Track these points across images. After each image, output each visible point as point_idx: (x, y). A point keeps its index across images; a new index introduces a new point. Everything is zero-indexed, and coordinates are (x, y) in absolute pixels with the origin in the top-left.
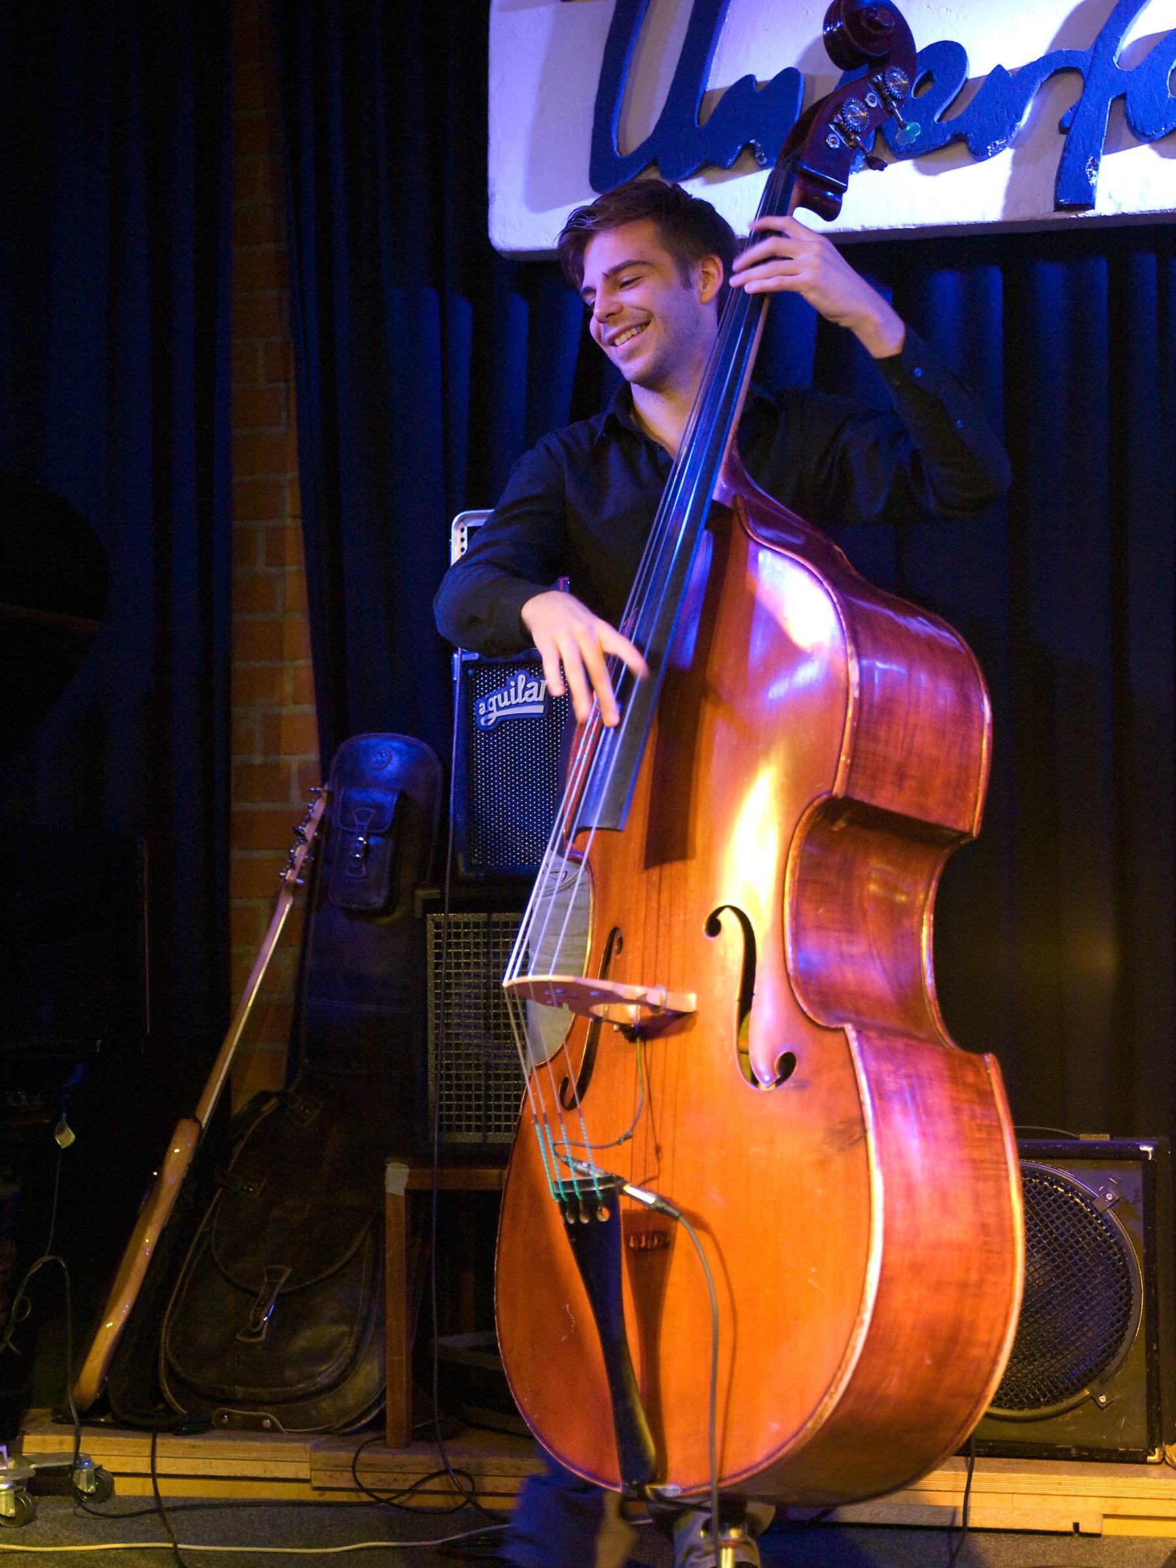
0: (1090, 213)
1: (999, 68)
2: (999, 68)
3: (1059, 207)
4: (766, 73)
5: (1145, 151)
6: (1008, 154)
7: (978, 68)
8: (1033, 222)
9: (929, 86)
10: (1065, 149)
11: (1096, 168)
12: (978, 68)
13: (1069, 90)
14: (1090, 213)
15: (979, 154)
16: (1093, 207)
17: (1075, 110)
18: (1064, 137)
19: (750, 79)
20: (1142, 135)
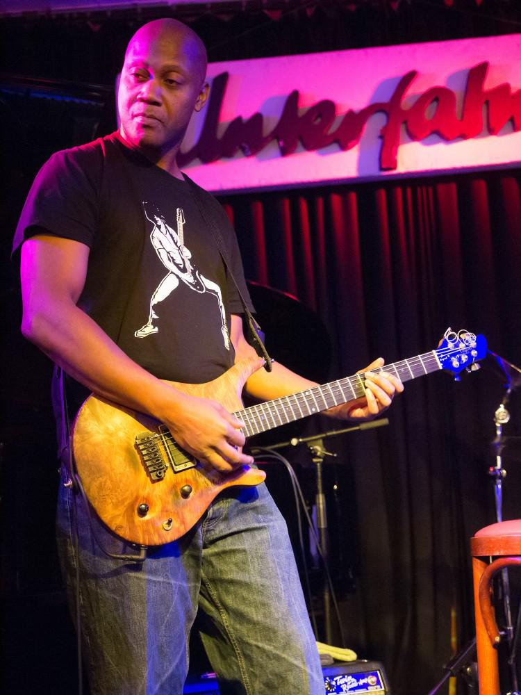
3: (381, 169)
4: (246, 116)
7: (343, 110)
9: (319, 121)
12: (343, 110)
14: (394, 172)
15: (344, 147)
16: (395, 168)
19: (239, 119)
20: (414, 137)
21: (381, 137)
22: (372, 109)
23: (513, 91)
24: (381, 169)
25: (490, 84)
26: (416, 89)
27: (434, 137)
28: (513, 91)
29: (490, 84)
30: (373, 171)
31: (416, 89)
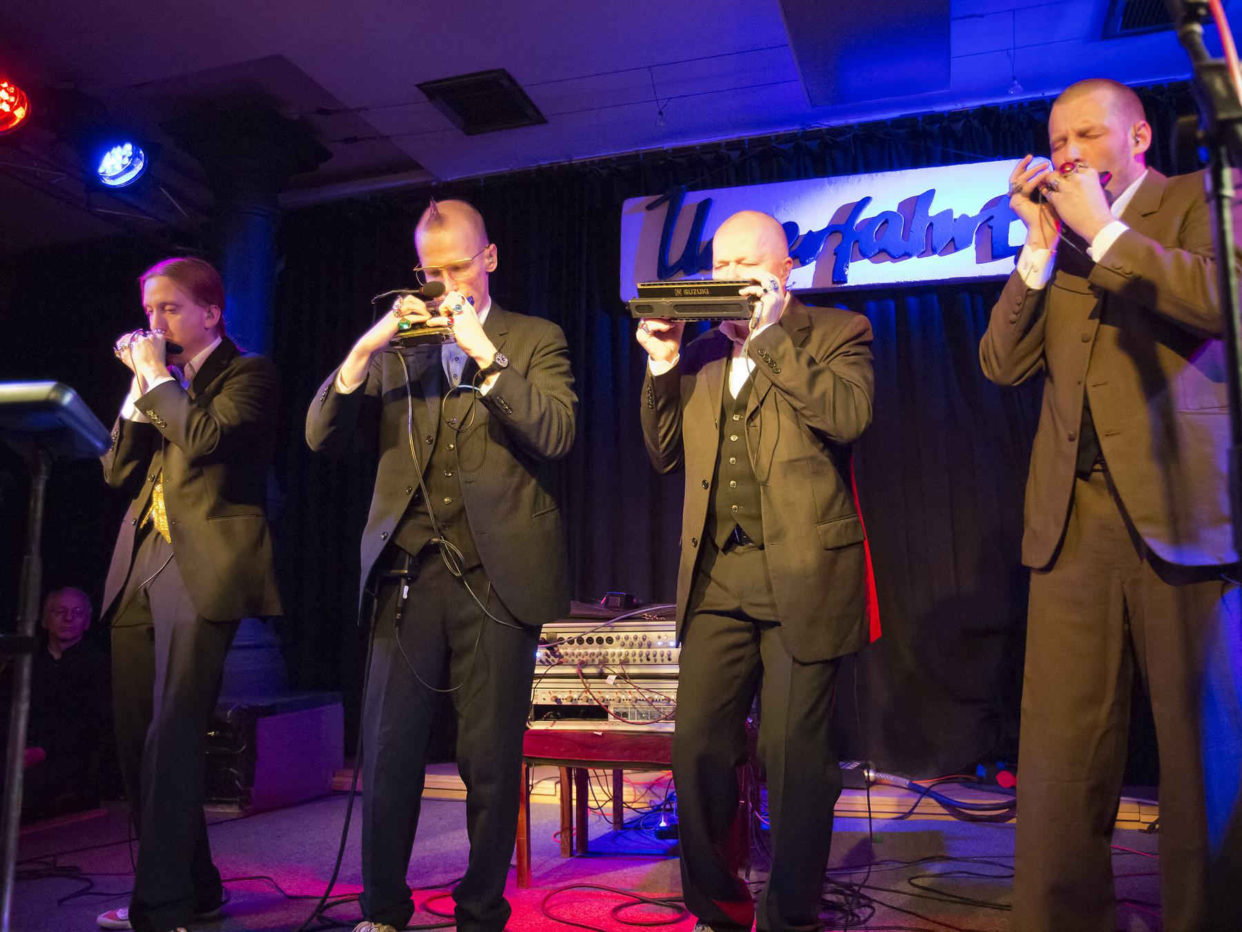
0: (845, 285)
1: (810, 231)
2: (810, 231)
3: (834, 282)
5: (866, 261)
6: (815, 262)
7: (803, 231)
8: (824, 289)
10: (836, 261)
11: (848, 267)
12: (803, 231)
13: (836, 240)
14: (845, 285)
17: (839, 246)
18: (835, 257)
20: (864, 256)
21: (835, 254)
22: (832, 229)
23: (956, 216)
24: (834, 282)
25: (934, 210)
26: (868, 213)
27: (884, 255)
28: (956, 216)
29: (934, 210)
30: (827, 283)
31: (868, 213)
